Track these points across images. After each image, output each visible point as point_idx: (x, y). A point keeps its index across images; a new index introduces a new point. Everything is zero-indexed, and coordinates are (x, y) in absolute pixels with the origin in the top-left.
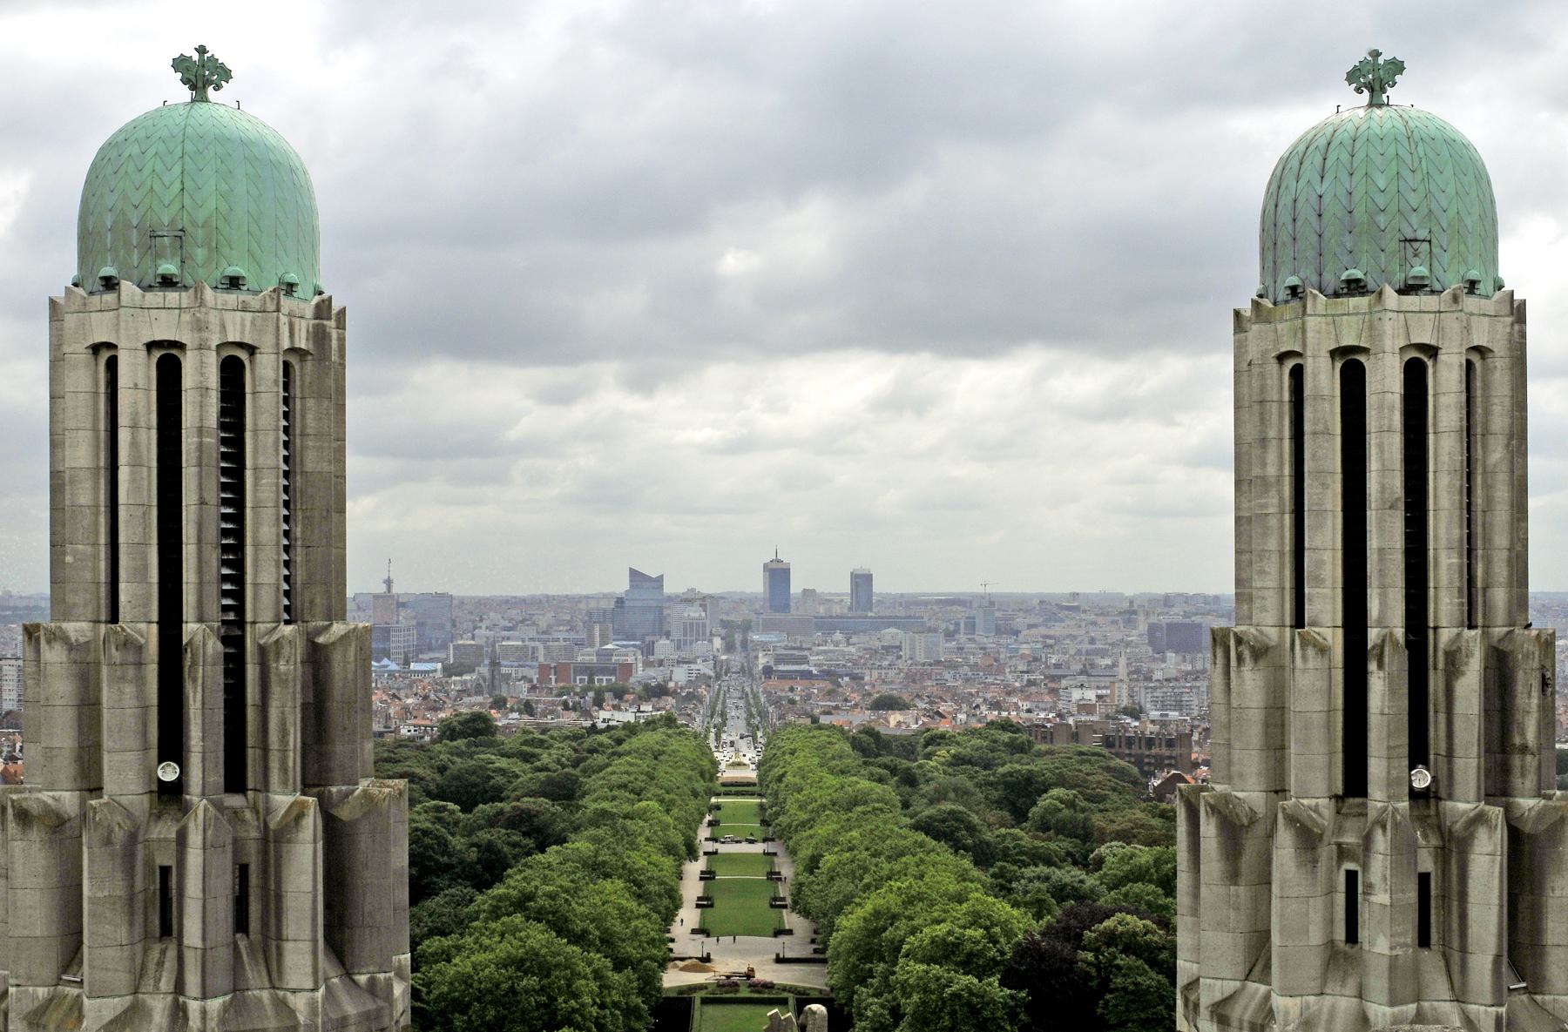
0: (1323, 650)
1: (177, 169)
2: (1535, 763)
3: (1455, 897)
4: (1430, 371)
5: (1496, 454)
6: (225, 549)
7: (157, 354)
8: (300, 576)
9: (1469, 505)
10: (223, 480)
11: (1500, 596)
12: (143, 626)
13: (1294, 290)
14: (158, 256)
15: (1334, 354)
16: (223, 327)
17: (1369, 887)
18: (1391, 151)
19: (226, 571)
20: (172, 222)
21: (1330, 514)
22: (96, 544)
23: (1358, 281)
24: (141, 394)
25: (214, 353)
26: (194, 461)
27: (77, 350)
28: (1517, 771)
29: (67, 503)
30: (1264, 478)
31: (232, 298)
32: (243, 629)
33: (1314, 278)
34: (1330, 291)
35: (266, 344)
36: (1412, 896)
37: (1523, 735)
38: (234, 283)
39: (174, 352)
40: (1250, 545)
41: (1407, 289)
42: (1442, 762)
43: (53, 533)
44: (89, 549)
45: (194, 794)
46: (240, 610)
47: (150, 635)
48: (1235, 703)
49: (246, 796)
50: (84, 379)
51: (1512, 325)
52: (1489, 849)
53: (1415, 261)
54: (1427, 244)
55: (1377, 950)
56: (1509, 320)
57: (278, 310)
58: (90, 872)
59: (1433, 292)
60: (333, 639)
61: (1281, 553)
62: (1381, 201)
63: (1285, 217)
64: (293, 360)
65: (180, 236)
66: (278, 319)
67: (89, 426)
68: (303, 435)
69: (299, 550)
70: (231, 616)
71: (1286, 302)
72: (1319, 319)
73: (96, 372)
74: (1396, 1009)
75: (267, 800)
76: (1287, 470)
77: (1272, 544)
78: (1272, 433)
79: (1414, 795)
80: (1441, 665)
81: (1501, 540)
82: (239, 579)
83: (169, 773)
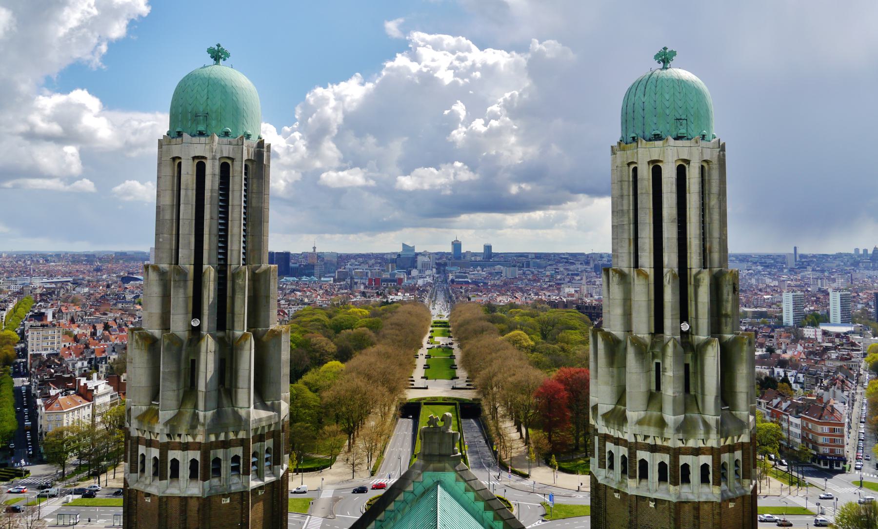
0: (646, 276)
1: (206, 91)
3: (699, 373)
4: (687, 169)
5: (714, 202)
6: (220, 236)
7: (197, 161)
8: (250, 247)
9: (703, 222)
11: (716, 256)
12: (187, 266)
13: (633, 138)
14: (198, 124)
15: (649, 163)
17: (665, 369)
19: (220, 245)
20: (203, 111)
21: (648, 225)
22: (172, 234)
23: (658, 135)
24: (189, 177)
25: (218, 161)
26: (208, 203)
27: (167, 159)
29: (161, 218)
31: (225, 140)
32: (227, 268)
33: (641, 134)
34: (648, 139)
35: (237, 157)
36: (682, 373)
37: (726, 310)
38: (227, 134)
39: (203, 160)
40: (617, 236)
41: (677, 138)
43: (156, 230)
45: (204, 332)
46: (226, 260)
47: (190, 269)
48: (611, 297)
49: (225, 332)
50: (168, 171)
51: (719, 152)
53: (681, 127)
54: (685, 121)
55: (668, 394)
56: (718, 150)
57: (243, 145)
58: (163, 362)
59: (688, 139)
60: (262, 271)
61: (630, 239)
63: (630, 110)
64: (249, 164)
65: (206, 116)
66: (243, 148)
67: (170, 188)
69: (249, 237)
70: (222, 262)
71: (631, 143)
72: (643, 149)
73: (174, 168)
74: (676, 417)
75: (233, 334)
76: (631, 208)
77: (626, 236)
78: (625, 193)
79: (682, 332)
80: (693, 283)
81: (716, 234)
82: (225, 248)
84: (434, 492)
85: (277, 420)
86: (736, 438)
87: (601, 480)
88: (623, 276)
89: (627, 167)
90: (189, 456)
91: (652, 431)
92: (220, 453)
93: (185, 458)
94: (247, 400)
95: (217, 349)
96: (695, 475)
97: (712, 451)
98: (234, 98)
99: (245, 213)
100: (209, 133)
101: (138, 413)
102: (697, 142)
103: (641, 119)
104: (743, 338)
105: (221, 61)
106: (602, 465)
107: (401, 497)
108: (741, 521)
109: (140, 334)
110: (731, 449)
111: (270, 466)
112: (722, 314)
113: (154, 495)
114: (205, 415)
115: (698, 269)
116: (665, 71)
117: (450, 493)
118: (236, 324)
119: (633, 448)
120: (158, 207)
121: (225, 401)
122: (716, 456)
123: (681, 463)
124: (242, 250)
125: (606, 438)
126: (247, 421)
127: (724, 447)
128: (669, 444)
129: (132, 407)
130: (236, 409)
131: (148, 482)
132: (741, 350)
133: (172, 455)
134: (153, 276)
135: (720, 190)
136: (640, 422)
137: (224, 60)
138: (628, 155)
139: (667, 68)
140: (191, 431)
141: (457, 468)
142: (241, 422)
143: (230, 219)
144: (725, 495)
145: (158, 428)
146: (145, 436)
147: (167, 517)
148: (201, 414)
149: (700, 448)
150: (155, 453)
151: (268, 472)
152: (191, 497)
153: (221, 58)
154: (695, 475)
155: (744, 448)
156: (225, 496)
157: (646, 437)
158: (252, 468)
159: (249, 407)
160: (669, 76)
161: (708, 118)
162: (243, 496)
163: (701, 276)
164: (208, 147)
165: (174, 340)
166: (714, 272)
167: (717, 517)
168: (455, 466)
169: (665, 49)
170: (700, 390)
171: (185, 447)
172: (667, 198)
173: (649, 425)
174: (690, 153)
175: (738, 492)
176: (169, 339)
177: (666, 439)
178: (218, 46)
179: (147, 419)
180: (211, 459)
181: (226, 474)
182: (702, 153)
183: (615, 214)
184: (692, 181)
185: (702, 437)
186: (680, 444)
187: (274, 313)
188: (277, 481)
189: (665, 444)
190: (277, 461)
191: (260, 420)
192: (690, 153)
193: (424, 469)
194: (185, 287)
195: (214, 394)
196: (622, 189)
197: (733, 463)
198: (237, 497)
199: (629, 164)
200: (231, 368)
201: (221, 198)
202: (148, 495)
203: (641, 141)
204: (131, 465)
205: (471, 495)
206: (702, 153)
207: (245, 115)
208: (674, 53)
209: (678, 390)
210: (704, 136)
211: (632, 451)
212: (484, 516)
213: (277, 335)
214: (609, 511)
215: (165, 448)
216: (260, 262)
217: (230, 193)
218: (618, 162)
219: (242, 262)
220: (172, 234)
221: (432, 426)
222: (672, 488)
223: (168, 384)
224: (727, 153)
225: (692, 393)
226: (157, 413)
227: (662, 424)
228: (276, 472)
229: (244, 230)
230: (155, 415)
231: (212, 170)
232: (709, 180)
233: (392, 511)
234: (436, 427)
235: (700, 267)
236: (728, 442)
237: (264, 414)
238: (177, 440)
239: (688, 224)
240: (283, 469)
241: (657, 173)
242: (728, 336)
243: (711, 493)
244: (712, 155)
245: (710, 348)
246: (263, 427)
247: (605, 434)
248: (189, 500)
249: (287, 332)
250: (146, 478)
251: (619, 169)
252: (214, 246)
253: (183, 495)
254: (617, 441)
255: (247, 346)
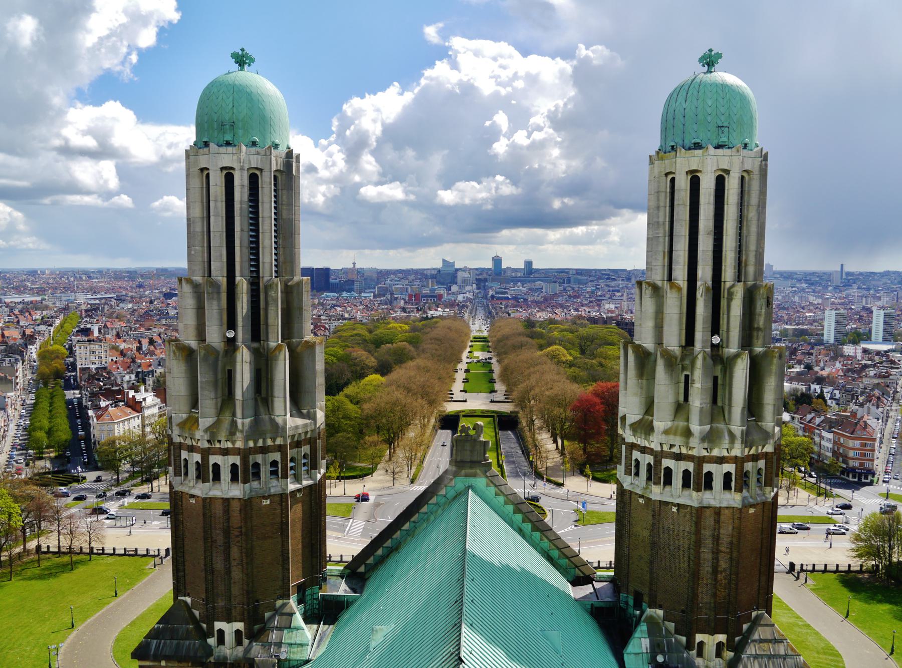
0: (679, 289)
1: (231, 99)
2: (763, 334)
5: (752, 214)
6: (252, 248)
7: (225, 172)
8: (281, 259)
9: (740, 235)
10: (251, 222)
11: (751, 270)
12: (220, 278)
13: (673, 147)
14: (224, 133)
15: (687, 173)
16: (250, 161)
17: (693, 381)
18: (715, 90)
21: (683, 237)
22: (203, 247)
23: (698, 143)
24: (218, 188)
26: (238, 214)
27: (196, 170)
28: (755, 338)
30: (658, 222)
31: (253, 150)
33: (681, 142)
34: (687, 147)
35: (266, 168)
36: (710, 385)
37: (758, 325)
38: (254, 144)
39: (231, 171)
41: (718, 147)
42: (725, 335)
43: (188, 243)
44: (200, 249)
46: (258, 272)
47: (223, 281)
48: (643, 310)
50: (197, 182)
52: (742, 367)
56: (760, 159)
59: (729, 148)
61: (664, 252)
62: (709, 110)
64: (278, 175)
65: (233, 125)
67: (200, 200)
68: (282, 204)
70: (255, 275)
71: (670, 152)
75: (268, 345)
76: (667, 219)
77: (661, 248)
78: (662, 204)
79: (713, 345)
80: (726, 296)
82: (257, 260)
83: (231, 334)
84: (465, 496)
85: (313, 427)
86: (760, 448)
87: (626, 486)
88: (656, 289)
89: (664, 178)
90: (230, 460)
91: (678, 440)
92: (259, 458)
93: (225, 463)
94: (283, 408)
95: (253, 358)
96: (718, 482)
97: (735, 460)
98: (261, 107)
99: (275, 225)
100: (236, 143)
101: (180, 421)
102: (738, 151)
103: (681, 126)
104: (773, 351)
105: (246, 66)
106: (628, 472)
107: (434, 500)
108: (760, 526)
109: (177, 346)
110: (755, 458)
111: (307, 470)
112: (754, 328)
113: (198, 497)
114: (243, 422)
115: (733, 283)
116: (708, 75)
117: (480, 497)
118: (270, 336)
119: (659, 456)
120: (188, 220)
121: (262, 410)
122: (739, 465)
123: (705, 471)
124: (274, 263)
125: (632, 446)
126: (284, 428)
127: (748, 456)
128: (694, 452)
129: (173, 415)
130: (273, 417)
131: (191, 484)
132: (771, 363)
133: (213, 459)
134: (187, 289)
135: (759, 202)
136: (666, 432)
137: (249, 65)
138: (667, 165)
139: (711, 72)
140: (230, 437)
141: (488, 474)
142: (278, 430)
143: (260, 231)
144: (746, 501)
145: (199, 434)
146: (187, 442)
147: (211, 516)
148: (239, 421)
149: (723, 457)
150: (197, 457)
151: (306, 476)
152: (233, 499)
153: (246, 63)
154: (718, 482)
155: (768, 457)
156: (264, 497)
157: (672, 446)
158: (290, 472)
159: (285, 415)
160: (713, 80)
161: (751, 125)
162: (282, 497)
163: (735, 289)
164: (235, 157)
165: (210, 350)
166: (749, 286)
167: (737, 521)
168: (486, 472)
169: (711, 50)
170: (727, 402)
171: (225, 452)
172: (704, 209)
173: (675, 434)
174: (731, 163)
175: (758, 499)
176: (205, 350)
177: (691, 448)
178: (243, 50)
179: (188, 425)
180: (251, 464)
181: (266, 478)
182: (743, 162)
183: (651, 226)
184: (731, 192)
185: (727, 446)
186: (705, 453)
187: (308, 326)
188: (315, 484)
189: (690, 453)
190: (314, 466)
191: (297, 427)
192: (731, 163)
193: (456, 475)
194: (219, 299)
195: (251, 403)
196: (658, 200)
197: (755, 472)
198: (277, 499)
199: (667, 174)
200: (267, 379)
201: (250, 210)
202: (193, 496)
203: (680, 150)
204: (175, 469)
205: (501, 499)
206: (743, 162)
207: (272, 123)
208: (719, 56)
209: (705, 401)
210: (746, 145)
211: (657, 459)
212: (513, 518)
213: (311, 346)
214: (633, 515)
215: (205, 453)
216: (292, 273)
217: (260, 204)
218: (656, 171)
219: (274, 274)
220: (203, 247)
221: (463, 434)
222: (694, 494)
223: (206, 393)
224: (769, 163)
225: (720, 404)
226: (197, 421)
227: (688, 433)
228: (313, 476)
229: (275, 243)
230: (195, 423)
231: (241, 181)
232: (749, 192)
233: (426, 513)
234: (468, 435)
235: (734, 280)
236: (753, 452)
237: (300, 422)
238: (218, 445)
239: (724, 237)
240: (320, 473)
241: (695, 183)
242: (759, 350)
243: (733, 499)
244: (753, 164)
245: (739, 361)
246: (300, 434)
247: (632, 443)
248: (231, 501)
249: (321, 343)
250: (190, 481)
251: (656, 179)
252: (246, 258)
253: (225, 497)
254: (644, 450)
255: (281, 357)
